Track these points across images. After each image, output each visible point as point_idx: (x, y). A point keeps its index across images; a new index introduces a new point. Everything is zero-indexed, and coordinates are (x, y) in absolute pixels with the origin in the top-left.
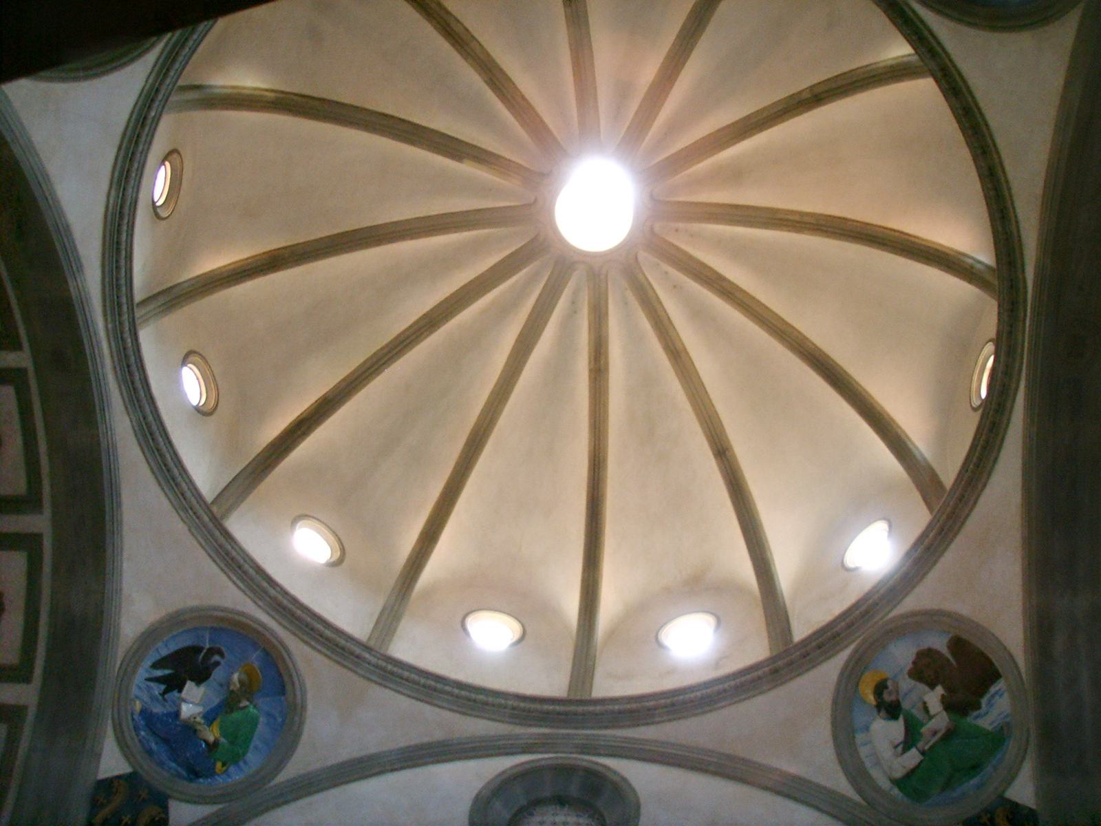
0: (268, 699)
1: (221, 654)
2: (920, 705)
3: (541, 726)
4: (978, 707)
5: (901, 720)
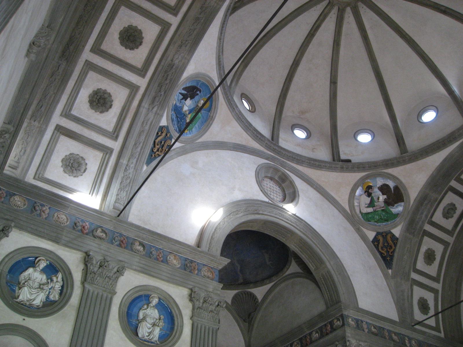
0: (205, 112)
1: (200, 92)
2: (377, 197)
3: (272, 152)
4: (394, 206)
5: (370, 198)
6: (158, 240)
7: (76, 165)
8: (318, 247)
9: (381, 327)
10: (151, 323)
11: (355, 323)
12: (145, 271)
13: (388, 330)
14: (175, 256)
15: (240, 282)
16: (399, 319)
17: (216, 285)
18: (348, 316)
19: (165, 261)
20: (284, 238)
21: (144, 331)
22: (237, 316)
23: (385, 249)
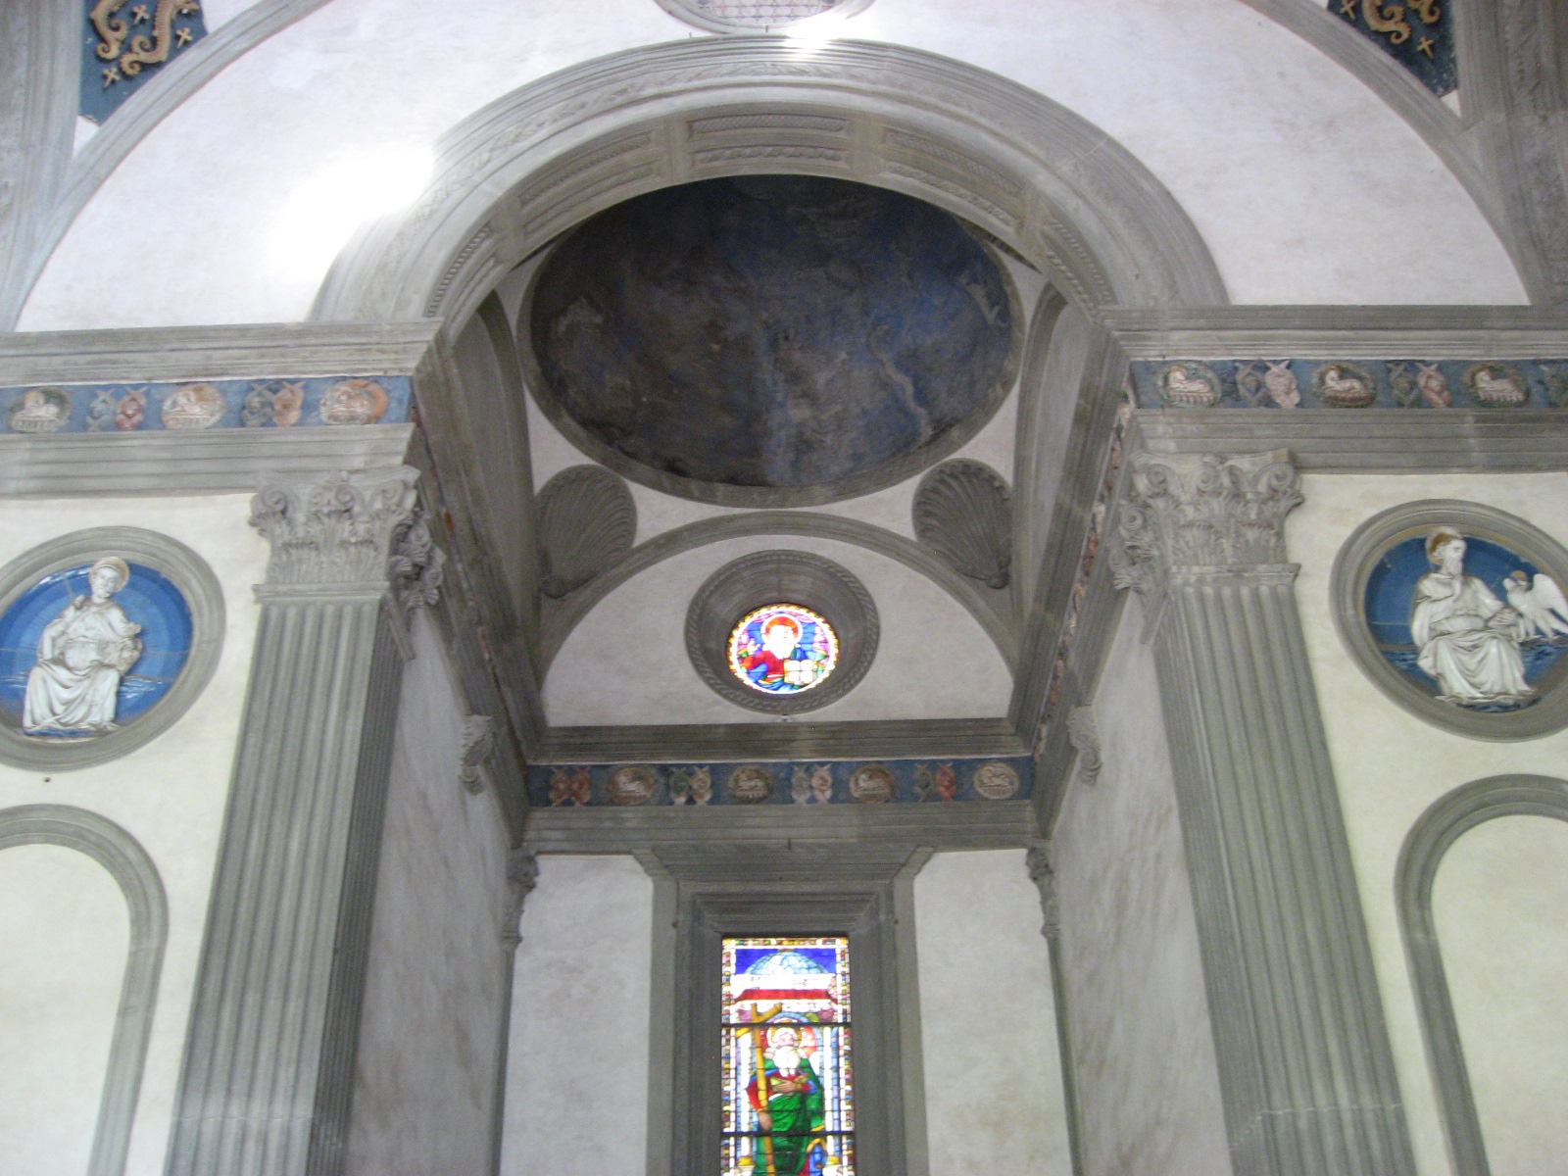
6: (116, 356)
8: (985, 129)
9: (1398, 363)
10: (88, 664)
11: (1212, 389)
12: (57, 487)
13: (1441, 367)
14: (198, 390)
15: (922, 440)
17: (380, 436)
18: (1165, 363)
19: (151, 419)
20: (832, 158)
22: (955, 578)
23: (1398, 10)
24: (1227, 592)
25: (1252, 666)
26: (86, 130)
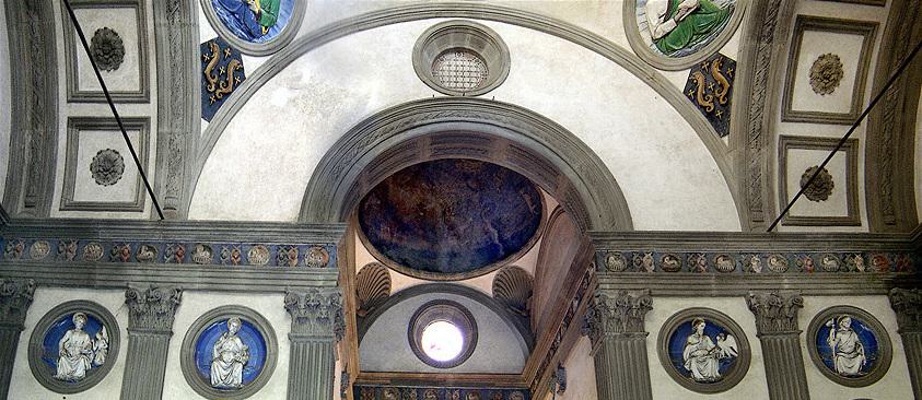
7: (108, 165)
16: (742, 227)
19: (244, 261)
21: (218, 373)
24: (623, 343)
25: (629, 369)
26: (205, 124)
